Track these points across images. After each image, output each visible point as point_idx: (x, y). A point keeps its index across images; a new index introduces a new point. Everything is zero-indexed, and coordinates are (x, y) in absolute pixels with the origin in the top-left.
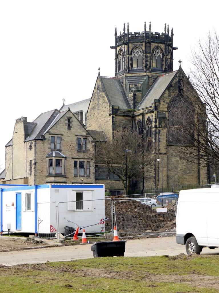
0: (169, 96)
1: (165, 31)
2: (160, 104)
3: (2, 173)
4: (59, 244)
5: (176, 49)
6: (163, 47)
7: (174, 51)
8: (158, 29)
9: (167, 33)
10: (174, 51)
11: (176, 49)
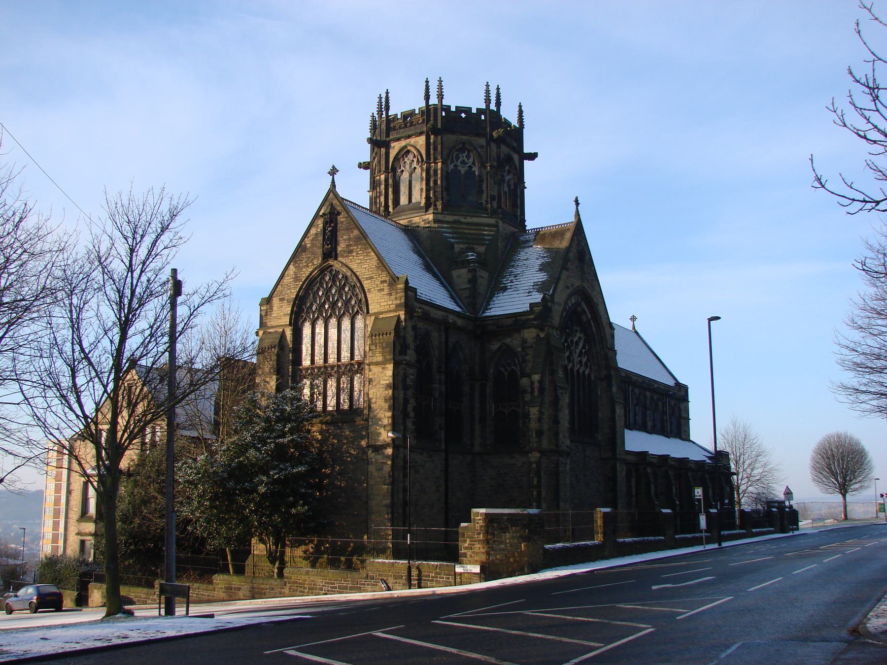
0: (296, 279)
1: (488, 101)
2: (271, 308)
3: (641, 339)
4: (222, 595)
5: (533, 156)
6: (421, 142)
7: (526, 162)
8: (464, 96)
9: (493, 107)
10: (526, 162)
11: (533, 156)
